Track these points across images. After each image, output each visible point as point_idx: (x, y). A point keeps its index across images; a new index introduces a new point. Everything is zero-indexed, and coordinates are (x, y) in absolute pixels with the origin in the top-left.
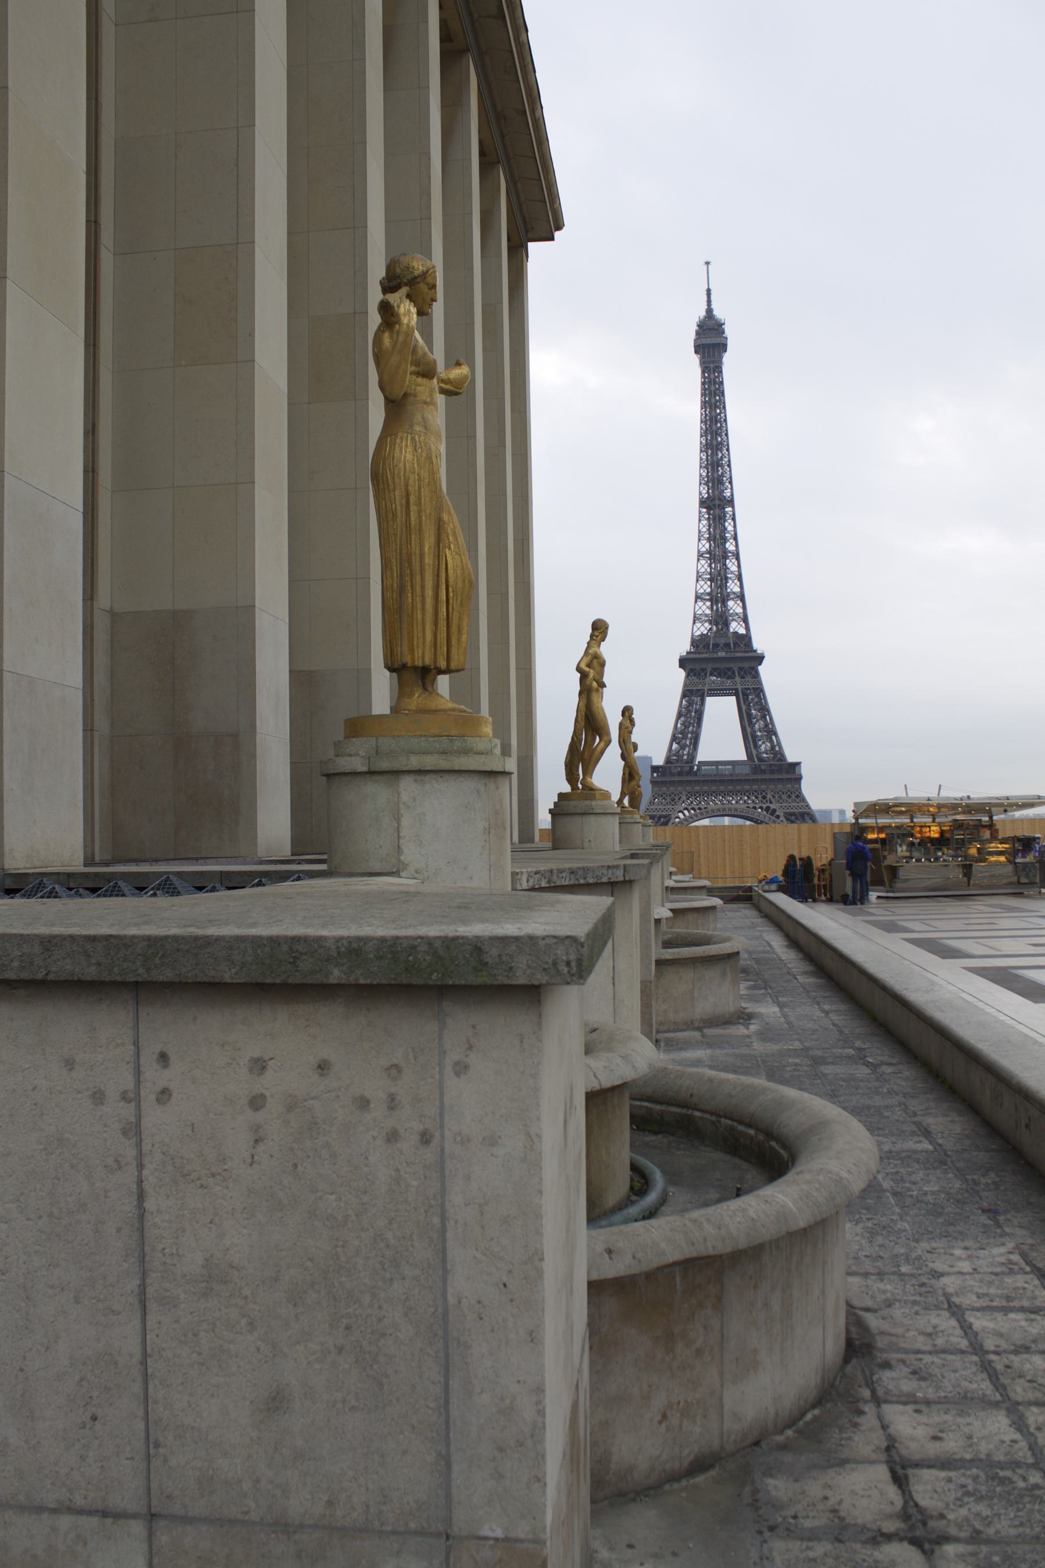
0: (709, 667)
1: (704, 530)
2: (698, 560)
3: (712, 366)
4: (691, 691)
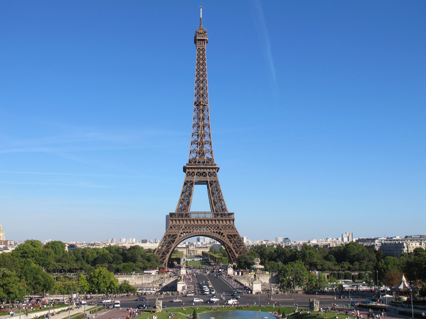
3: (201, 48)
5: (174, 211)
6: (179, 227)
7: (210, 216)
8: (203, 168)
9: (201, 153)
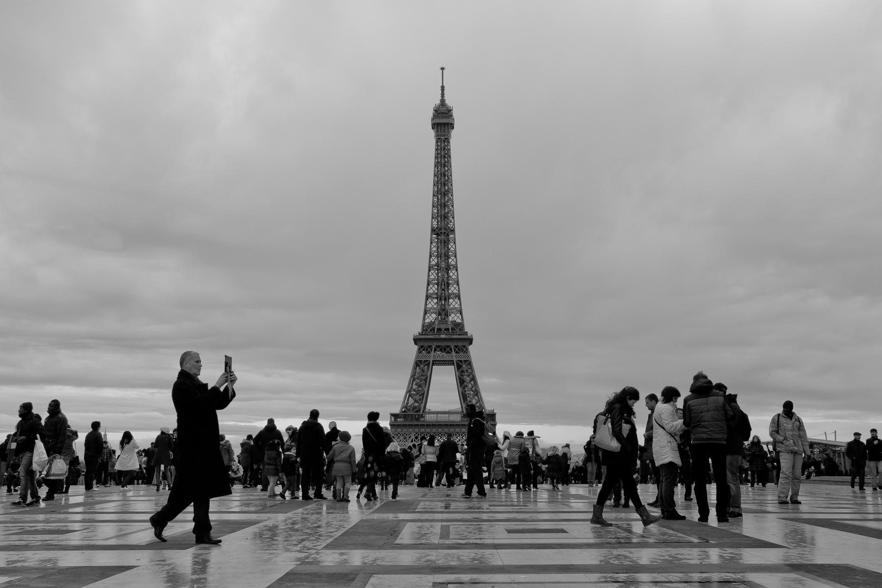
0: (434, 345)
1: (434, 249)
2: (430, 270)
4: (421, 361)
5: (397, 410)
7: (457, 418)
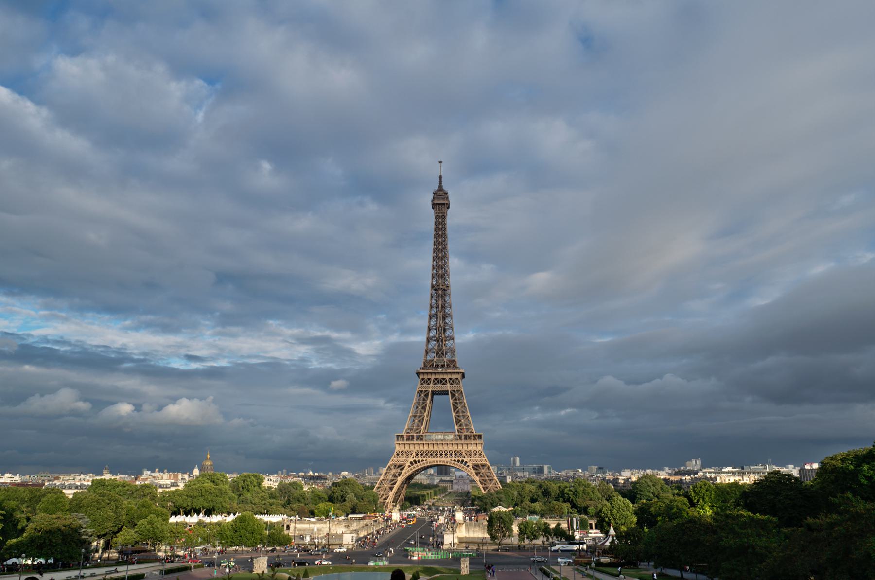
1: (434, 301)
4: (421, 391)
6: (408, 453)
8: (442, 373)
9: (440, 353)
